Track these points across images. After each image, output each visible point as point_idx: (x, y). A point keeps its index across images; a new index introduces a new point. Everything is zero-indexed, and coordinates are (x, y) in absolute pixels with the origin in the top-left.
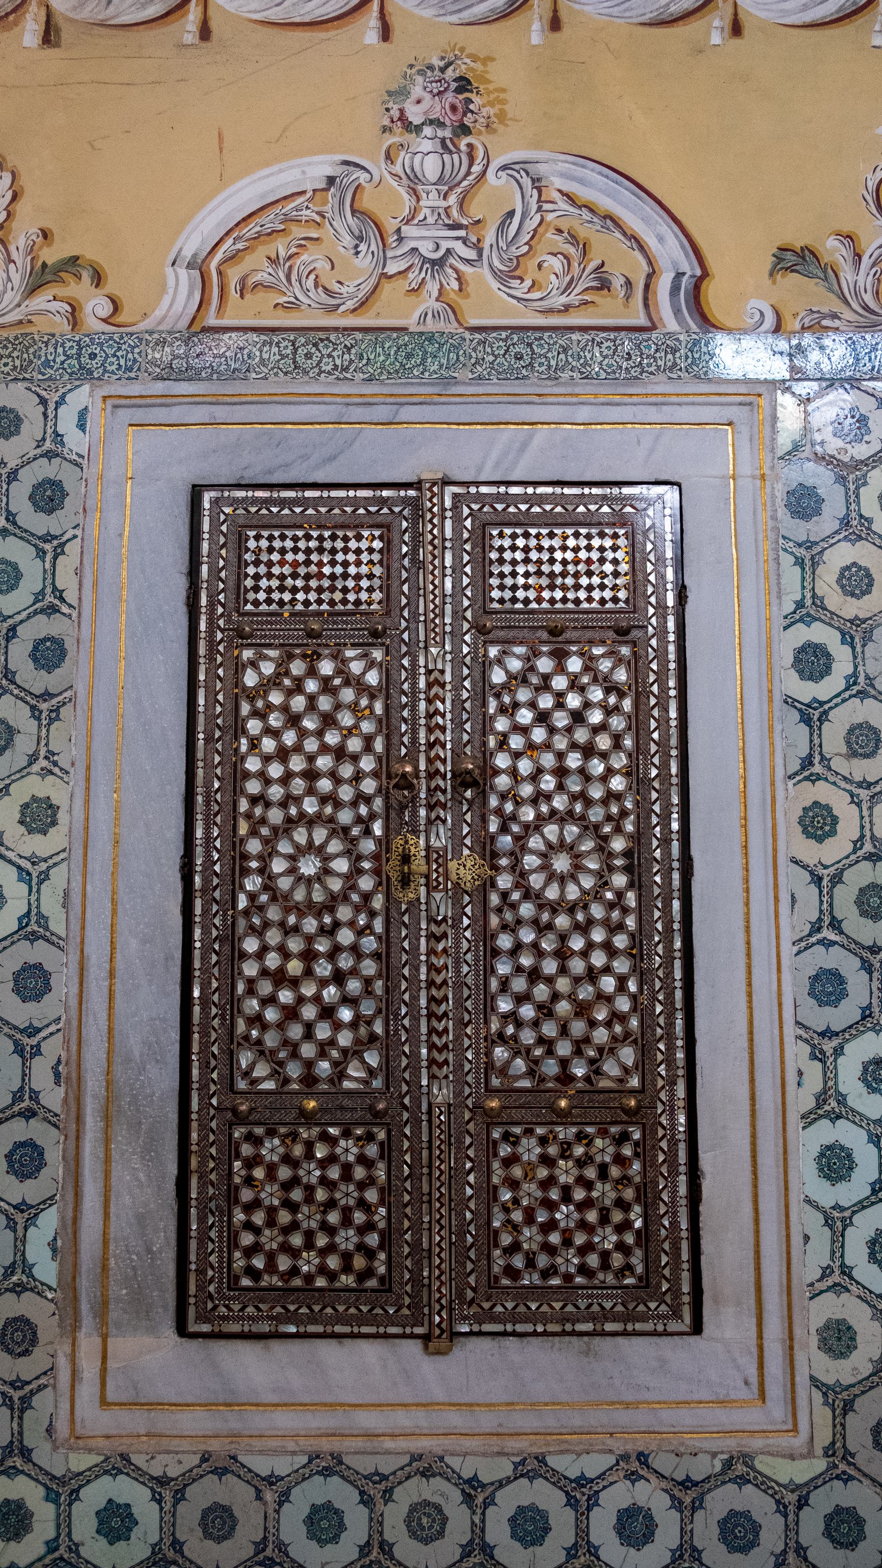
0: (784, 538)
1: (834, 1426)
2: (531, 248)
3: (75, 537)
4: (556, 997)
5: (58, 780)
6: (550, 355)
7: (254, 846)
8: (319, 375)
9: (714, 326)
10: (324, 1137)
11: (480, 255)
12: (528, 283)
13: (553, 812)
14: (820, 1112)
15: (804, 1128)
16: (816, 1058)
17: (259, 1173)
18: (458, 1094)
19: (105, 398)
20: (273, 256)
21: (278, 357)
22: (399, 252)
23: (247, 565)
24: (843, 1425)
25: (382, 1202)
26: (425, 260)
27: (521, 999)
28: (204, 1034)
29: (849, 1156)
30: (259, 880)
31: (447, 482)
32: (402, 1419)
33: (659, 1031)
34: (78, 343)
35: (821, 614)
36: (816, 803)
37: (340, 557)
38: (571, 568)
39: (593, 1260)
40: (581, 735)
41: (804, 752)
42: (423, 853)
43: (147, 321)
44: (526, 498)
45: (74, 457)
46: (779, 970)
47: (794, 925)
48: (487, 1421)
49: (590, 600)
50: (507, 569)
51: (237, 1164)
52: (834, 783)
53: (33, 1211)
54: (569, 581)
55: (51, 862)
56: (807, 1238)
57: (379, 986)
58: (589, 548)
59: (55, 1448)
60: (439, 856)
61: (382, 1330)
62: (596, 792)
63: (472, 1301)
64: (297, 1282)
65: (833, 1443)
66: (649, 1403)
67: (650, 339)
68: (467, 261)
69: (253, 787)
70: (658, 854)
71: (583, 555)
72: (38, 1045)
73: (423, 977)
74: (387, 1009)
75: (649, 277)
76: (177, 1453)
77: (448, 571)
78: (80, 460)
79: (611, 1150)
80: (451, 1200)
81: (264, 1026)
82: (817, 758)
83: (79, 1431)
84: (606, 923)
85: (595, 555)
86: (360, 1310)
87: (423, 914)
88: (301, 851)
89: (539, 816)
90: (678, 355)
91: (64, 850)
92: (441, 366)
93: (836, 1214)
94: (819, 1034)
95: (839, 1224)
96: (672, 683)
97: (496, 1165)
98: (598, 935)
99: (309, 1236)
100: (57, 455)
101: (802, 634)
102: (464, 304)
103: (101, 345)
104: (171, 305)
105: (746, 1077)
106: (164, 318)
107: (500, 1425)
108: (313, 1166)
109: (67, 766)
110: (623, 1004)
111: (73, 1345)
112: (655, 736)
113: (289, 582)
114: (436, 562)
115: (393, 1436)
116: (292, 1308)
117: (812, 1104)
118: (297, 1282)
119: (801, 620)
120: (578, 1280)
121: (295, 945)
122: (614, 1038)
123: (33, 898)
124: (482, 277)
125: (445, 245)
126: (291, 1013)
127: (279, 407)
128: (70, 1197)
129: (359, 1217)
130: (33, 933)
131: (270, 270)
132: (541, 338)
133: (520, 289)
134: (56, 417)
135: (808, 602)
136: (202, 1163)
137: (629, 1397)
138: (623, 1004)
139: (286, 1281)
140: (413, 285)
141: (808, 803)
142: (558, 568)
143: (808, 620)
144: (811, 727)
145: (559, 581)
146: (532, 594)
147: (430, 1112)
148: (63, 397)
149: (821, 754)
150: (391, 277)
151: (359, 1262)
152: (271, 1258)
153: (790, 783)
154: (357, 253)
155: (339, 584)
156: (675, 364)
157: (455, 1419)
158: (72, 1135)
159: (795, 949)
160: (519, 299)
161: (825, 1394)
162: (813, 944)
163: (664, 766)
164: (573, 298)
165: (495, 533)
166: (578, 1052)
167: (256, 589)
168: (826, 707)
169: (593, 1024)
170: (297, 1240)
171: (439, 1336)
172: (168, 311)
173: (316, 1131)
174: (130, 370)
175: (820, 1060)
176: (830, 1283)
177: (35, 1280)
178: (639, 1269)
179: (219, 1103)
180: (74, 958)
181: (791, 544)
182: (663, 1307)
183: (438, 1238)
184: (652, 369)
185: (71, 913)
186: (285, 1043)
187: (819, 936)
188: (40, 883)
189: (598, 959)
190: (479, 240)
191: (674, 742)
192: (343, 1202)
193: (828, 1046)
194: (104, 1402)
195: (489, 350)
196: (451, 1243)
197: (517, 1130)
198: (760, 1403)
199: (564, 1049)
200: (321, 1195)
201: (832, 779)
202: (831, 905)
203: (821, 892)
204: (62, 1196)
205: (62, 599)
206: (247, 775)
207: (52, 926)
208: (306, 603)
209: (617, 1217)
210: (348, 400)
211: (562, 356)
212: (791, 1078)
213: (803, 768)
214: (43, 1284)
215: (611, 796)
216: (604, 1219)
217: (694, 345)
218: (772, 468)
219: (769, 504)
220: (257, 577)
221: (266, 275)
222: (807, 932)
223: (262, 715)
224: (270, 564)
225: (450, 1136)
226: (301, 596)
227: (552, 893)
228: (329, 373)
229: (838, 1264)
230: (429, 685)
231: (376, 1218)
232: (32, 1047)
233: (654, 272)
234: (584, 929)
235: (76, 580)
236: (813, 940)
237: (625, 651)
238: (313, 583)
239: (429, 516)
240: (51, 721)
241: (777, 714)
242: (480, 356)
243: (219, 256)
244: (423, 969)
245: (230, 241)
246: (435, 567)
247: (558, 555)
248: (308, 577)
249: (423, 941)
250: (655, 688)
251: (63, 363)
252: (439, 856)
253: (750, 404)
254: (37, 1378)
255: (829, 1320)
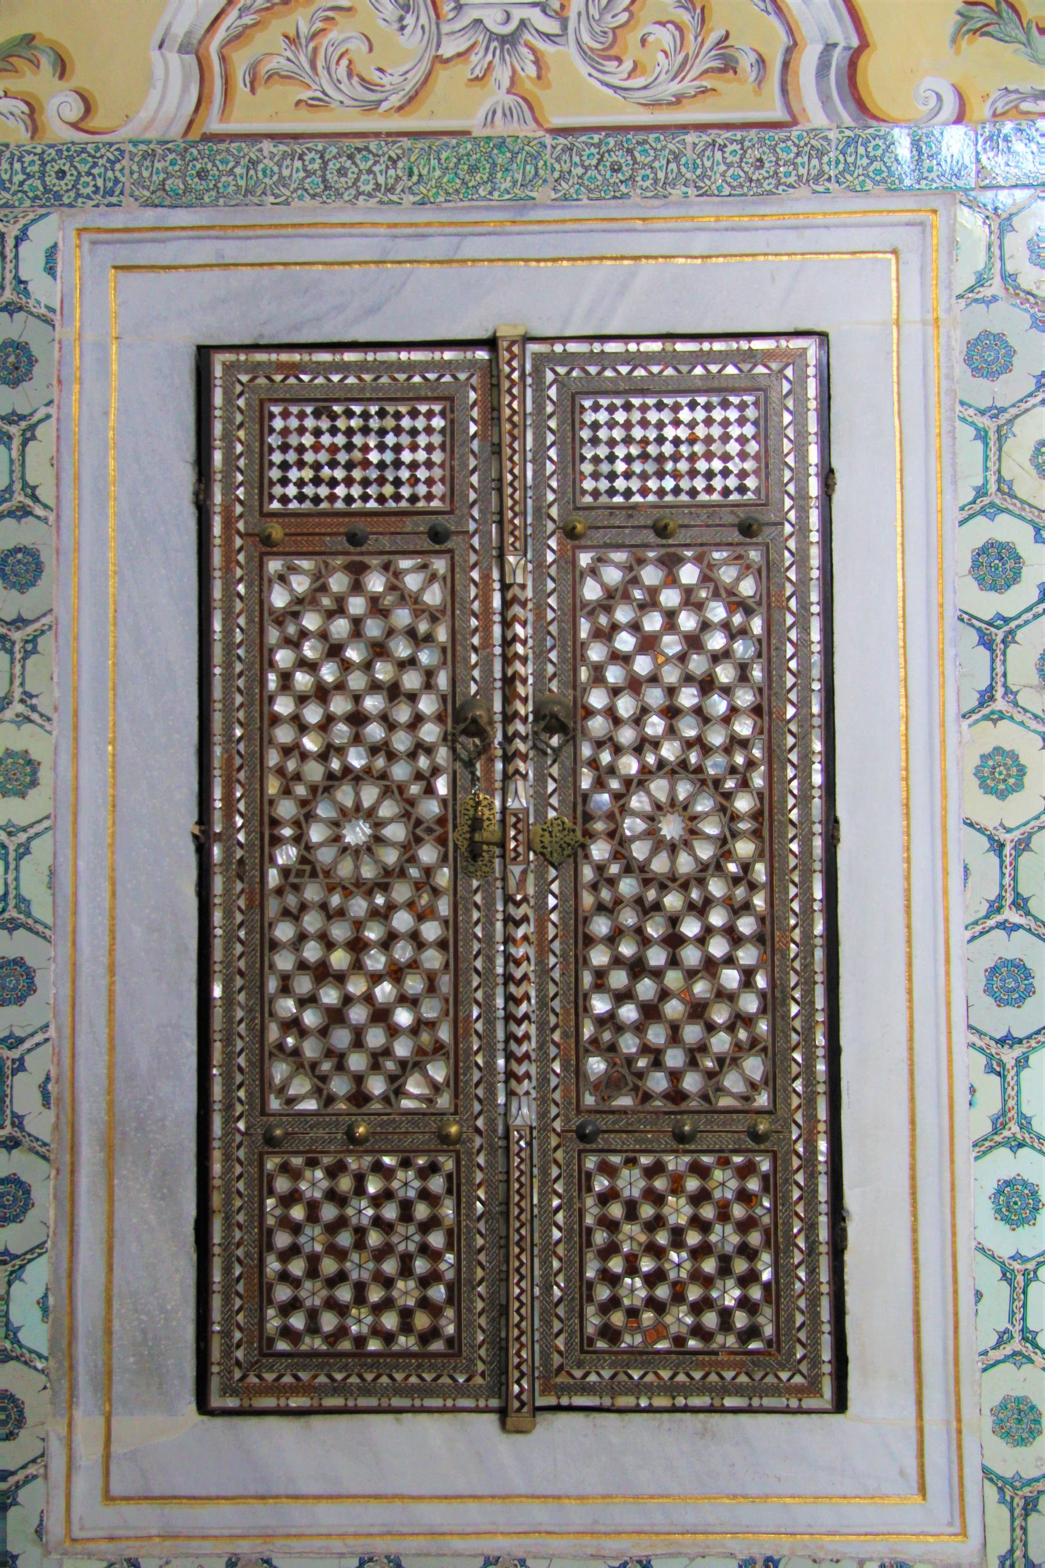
0: (962, 403)
1: (1013, 1530)
2: (632, 15)
3: (48, 417)
4: (664, 994)
5: (38, 729)
6: (656, 164)
7: (286, 809)
8: (356, 198)
9: (875, 117)
10: (377, 1167)
11: (564, 27)
12: (628, 65)
13: (661, 763)
14: (998, 1138)
15: (976, 1158)
16: (992, 1071)
17: (298, 1213)
18: (543, 1115)
19: (80, 231)
20: (292, 34)
21: (302, 174)
22: (458, 26)
23: (271, 450)
24: (1024, 1529)
25: (449, 1247)
26: (492, 36)
27: (622, 997)
28: (228, 1042)
29: (1034, 1193)
30: (293, 851)
31: (528, 339)
32: (474, 1514)
33: (795, 1037)
34: (41, 156)
35: (1008, 504)
36: (998, 750)
37: (390, 440)
38: (684, 449)
39: (710, 1320)
40: (697, 664)
41: (984, 684)
42: (498, 817)
43: (130, 126)
44: (627, 358)
45: (43, 311)
46: (947, 961)
47: (967, 904)
48: (577, 1516)
49: (709, 490)
50: (603, 451)
51: (270, 1202)
52: (1022, 723)
53: (18, 1262)
54: (683, 466)
55: (32, 832)
56: (979, 1295)
57: (445, 983)
58: (709, 422)
59: (47, 1553)
60: (519, 820)
61: (449, 1403)
62: (716, 738)
63: (561, 1368)
64: (346, 1345)
65: (1011, 1551)
66: (779, 1497)
67: (789, 138)
68: (548, 36)
69: (284, 735)
70: (794, 815)
71: (701, 431)
72: (21, 1060)
73: (500, 970)
74: (455, 1007)
75: (789, 51)
76: (197, 1556)
77: (529, 456)
78: (50, 315)
79: (733, 1184)
80: (532, 1245)
81: (303, 1033)
82: (1000, 691)
83: (77, 1533)
84: (728, 902)
85: (716, 431)
86: (423, 1379)
87: (499, 892)
88: (345, 815)
89: (644, 769)
90: (825, 159)
91: (48, 817)
92: (515, 182)
93: (1016, 1266)
94: (997, 1042)
95: (1020, 1278)
96: (814, 597)
97: (590, 1201)
98: (717, 918)
99: (360, 1289)
100: (20, 309)
101: (982, 531)
102: (545, 98)
103: (70, 159)
104: (161, 103)
105: (905, 1094)
106: (153, 120)
107: (596, 1522)
108: (364, 1203)
109: (48, 711)
110: (750, 1004)
111: (70, 1425)
112: (793, 665)
113: (326, 472)
114: (516, 445)
115: (463, 1534)
116: (339, 1377)
117: (988, 1128)
118: (346, 1345)
119: (982, 511)
120: (692, 1343)
121: (340, 932)
122: (738, 1046)
123: (11, 876)
124: (567, 60)
125: (518, 14)
126: (336, 1016)
127: (306, 241)
128: (65, 1242)
129: (421, 1266)
130: (12, 920)
131: (289, 54)
132: (645, 142)
133: (618, 73)
134: (16, 257)
135: (992, 487)
136: (227, 1202)
137: (753, 1489)
138: (750, 1004)
139: (332, 1344)
140: (477, 72)
141: (987, 749)
142: (668, 449)
143: (991, 511)
144: (992, 651)
145: (669, 466)
146: (635, 484)
147: (507, 1136)
148: (24, 231)
149: (1005, 685)
150: (448, 61)
151: (422, 1321)
152: (313, 1316)
153: (965, 723)
154: (403, 28)
155: (390, 475)
156: (822, 172)
157: (540, 1514)
158: (66, 1170)
159: (968, 934)
160: (615, 88)
161: (1001, 1490)
162: (991, 929)
163: (803, 704)
164: (687, 86)
165: (587, 403)
166: (693, 1063)
167: (284, 482)
168: (1013, 625)
169: (711, 1028)
170: (344, 1294)
171: (519, 1410)
172: (157, 111)
173: (368, 1160)
174: (110, 194)
175: (999, 1074)
176: (1008, 1350)
177: (21, 1346)
178: (768, 1331)
179: (248, 1128)
180: (64, 949)
181: (971, 412)
182: (798, 1379)
183: (517, 1291)
184: (792, 180)
185: (58, 895)
186: (329, 1053)
187: (999, 918)
188: (20, 857)
189: (718, 948)
190: (563, 7)
191: (816, 672)
192: (401, 1247)
193: (1009, 1056)
194: (108, 1497)
195: (576, 159)
196: (533, 1298)
197: (616, 1159)
198: (919, 1499)
199: (674, 1058)
200: (374, 1239)
201: (1018, 717)
202: (1015, 879)
203: (1002, 862)
204: (54, 1243)
205: (35, 498)
206: (276, 719)
207: (37, 911)
208: (349, 499)
209: (740, 1266)
210: (395, 231)
211: (673, 166)
212: (961, 1096)
213: (981, 704)
214: (31, 1351)
215: (737, 743)
216: (725, 1269)
217: (848, 145)
218: (949, 310)
219: (943, 359)
220: (285, 466)
221: (283, 61)
222: (983, 912)
223: (294, 643)
224: (301, 449)
225: (532, 1166)
226: (341, 491)
227: (660, 865)
228: (370, 195)
229: (1018, 1327)
230: (506, 604)
231: (443, 1266)
232: (14, 1061)
233: (795, 44)
234: (700, 909)
235: (51, 473)
236: (991, 923)
237: (754, 555)
238: (357, 474)
239: (506, 384)
240: (27, 655)
241: (949, 634)
242: (566, 167)
243: (221, 34)
244: (500, 960)
245: (234, 14)
246: (514, 452)
247: (669, 432)
248: (350, 466)
249: (499, 925)
250: (793, 604)
251: (21, 184)
252: (519, 820)
253: (921, 224)
254: (24, 1467)
255: (1006, 1399)
